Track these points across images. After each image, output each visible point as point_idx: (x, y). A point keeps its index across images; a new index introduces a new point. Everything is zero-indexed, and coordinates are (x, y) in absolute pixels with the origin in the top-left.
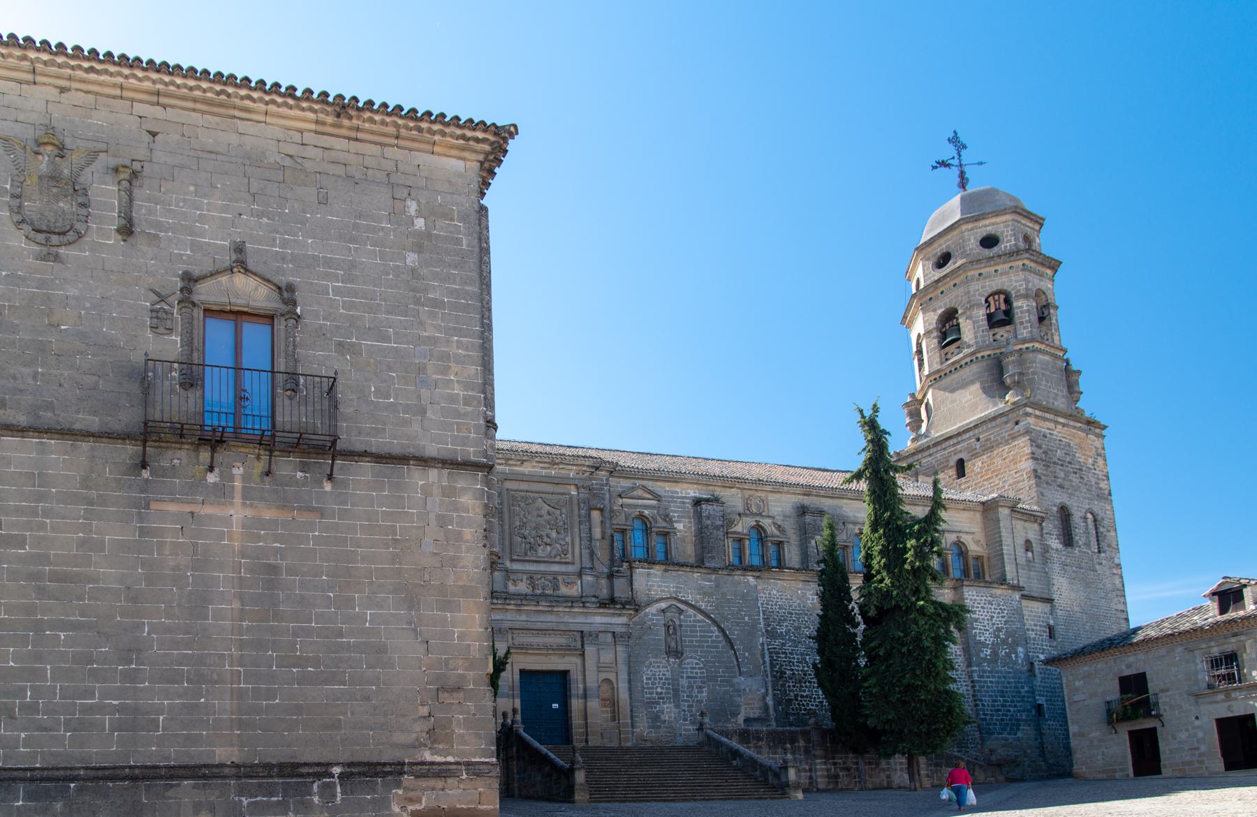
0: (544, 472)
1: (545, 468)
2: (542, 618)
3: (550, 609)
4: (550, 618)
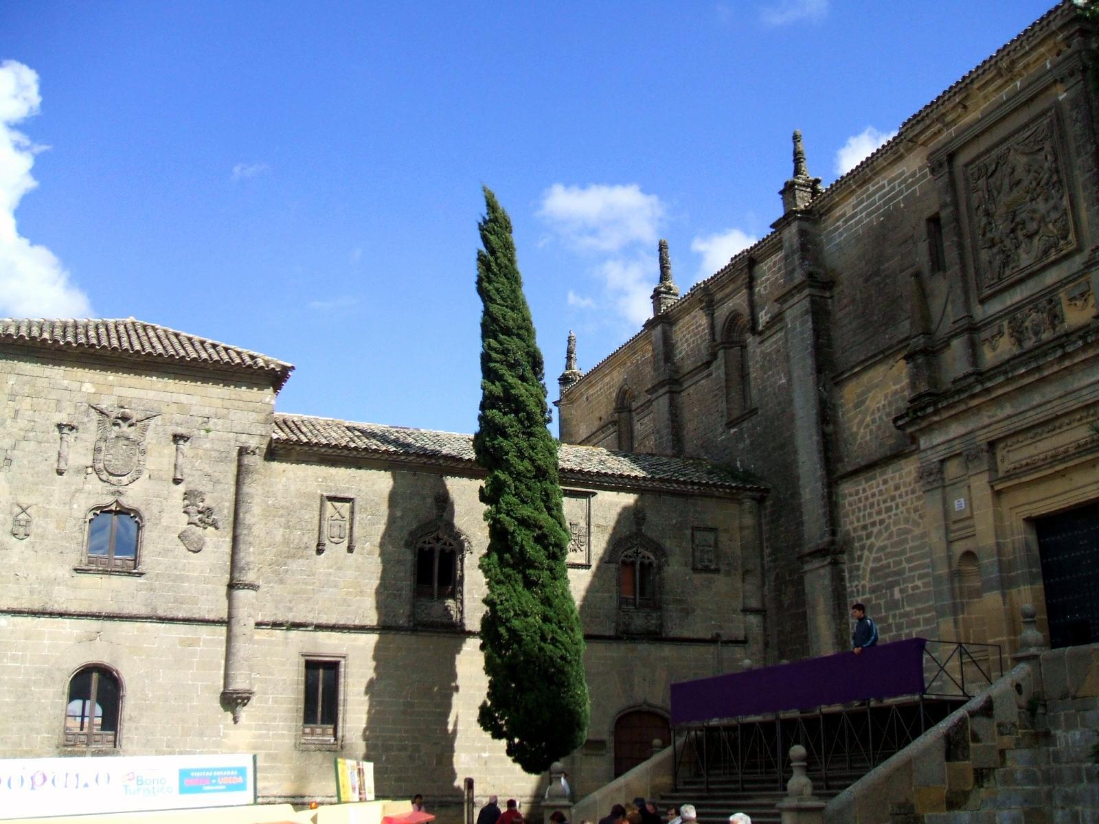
0: (1003, 95)
1: (1000, 88)
2: (1037, 399)
3: (1037, 376)
4: (1051, 391)
